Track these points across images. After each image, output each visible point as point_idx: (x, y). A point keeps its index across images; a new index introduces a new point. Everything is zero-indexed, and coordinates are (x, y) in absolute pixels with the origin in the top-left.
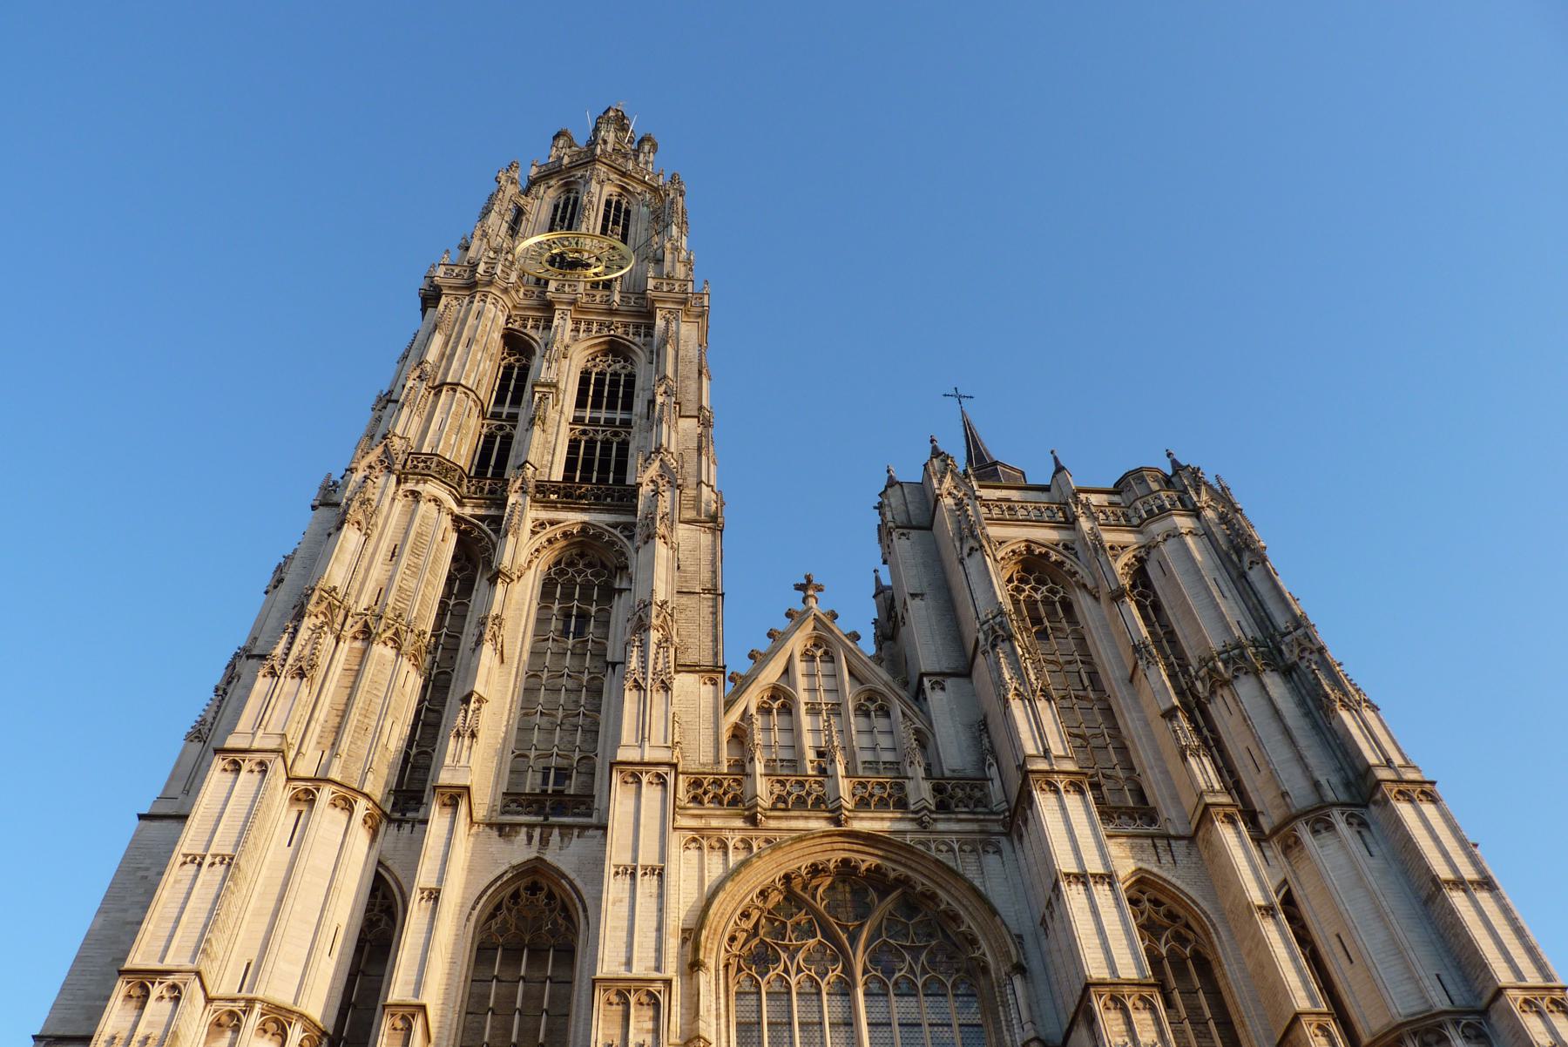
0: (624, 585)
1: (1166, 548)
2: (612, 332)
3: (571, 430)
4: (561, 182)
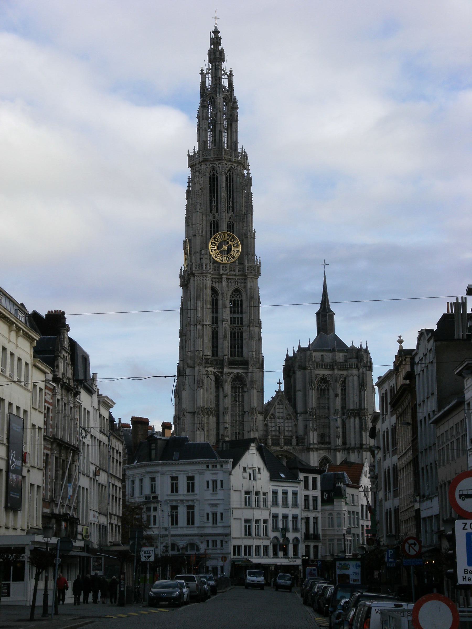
0: (245, 389)
1: (351, 378)
2: (237, 286)
3: (230, 328)
4: (211, 165)
